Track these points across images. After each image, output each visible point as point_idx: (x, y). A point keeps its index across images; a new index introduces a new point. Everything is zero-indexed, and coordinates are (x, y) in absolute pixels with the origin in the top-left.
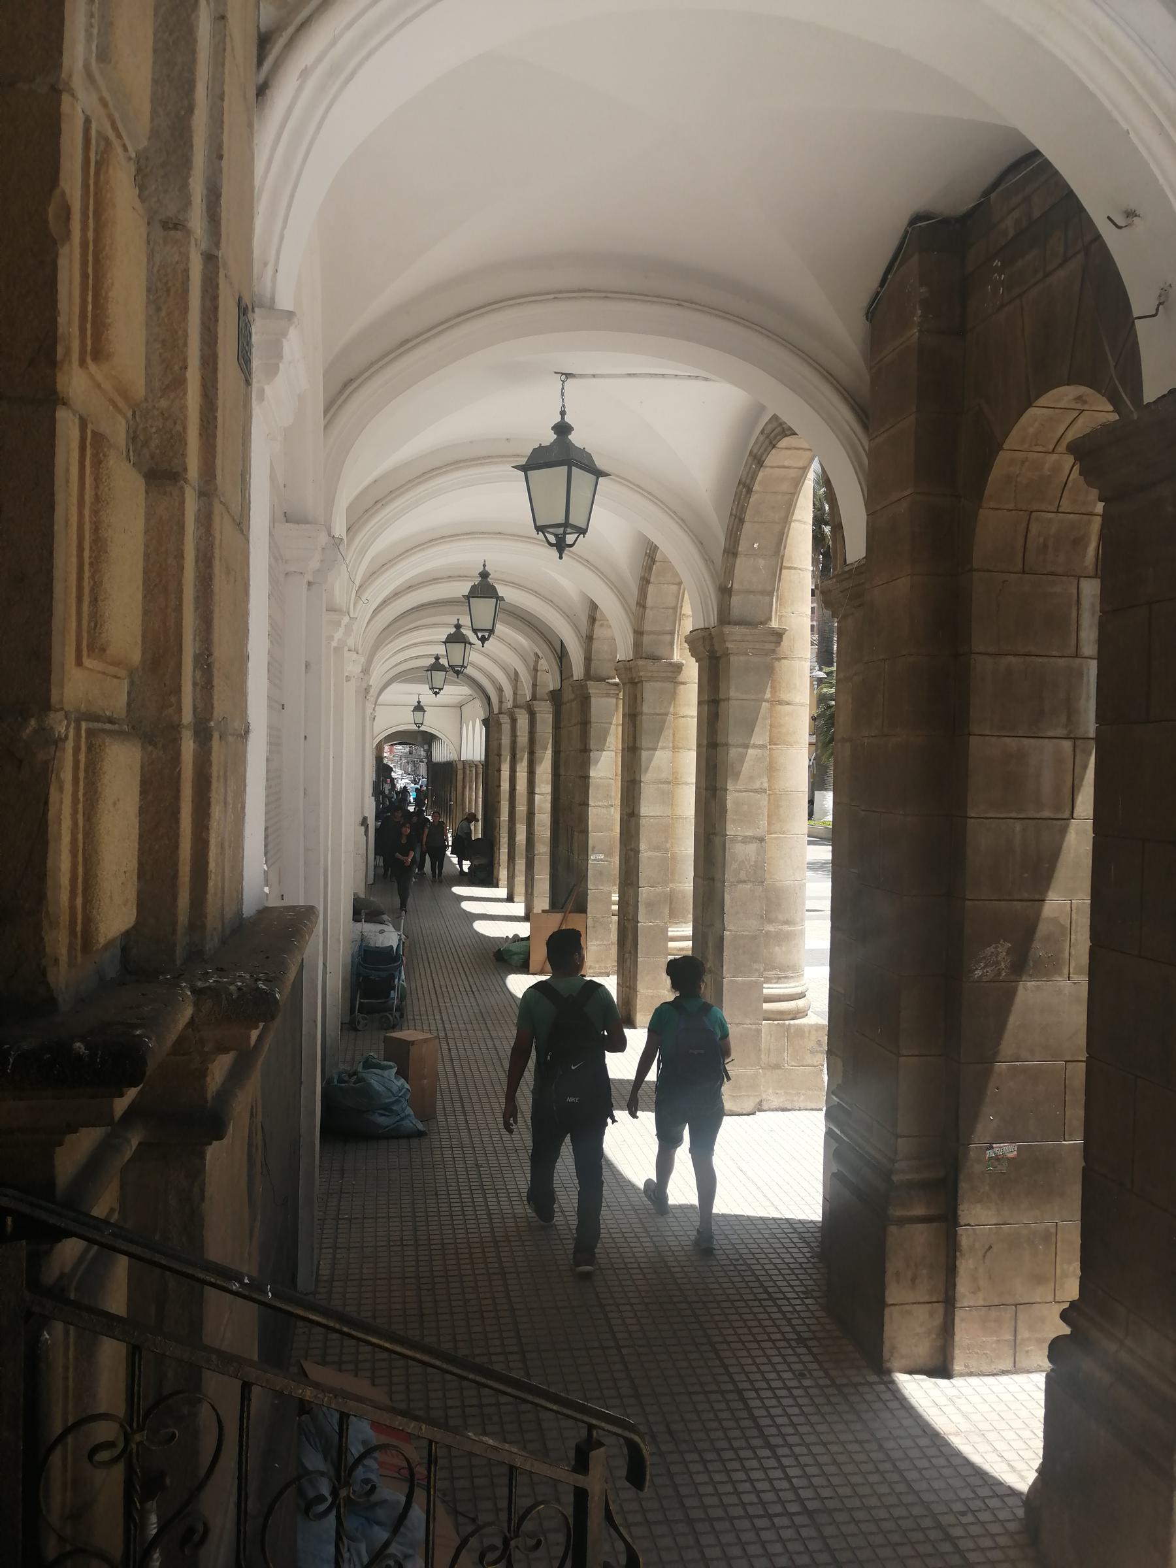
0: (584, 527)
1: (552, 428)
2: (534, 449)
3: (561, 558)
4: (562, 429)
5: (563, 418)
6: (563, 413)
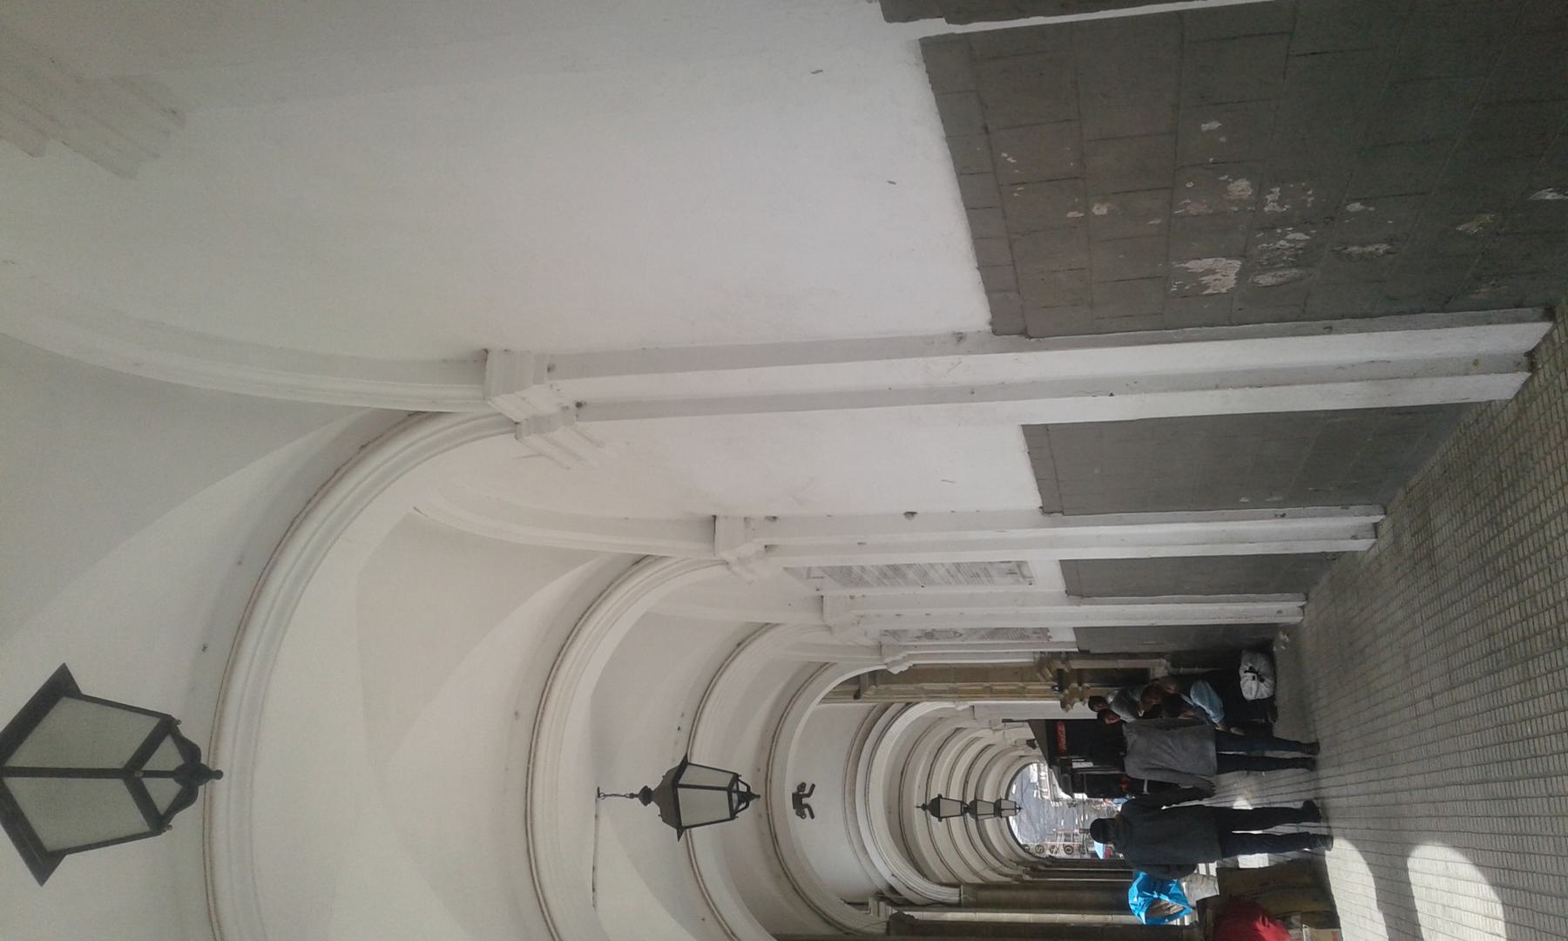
0: (731, 776)
1: (646, 805)
3: (759, 796)
4: (646, 796)
5: (636, 796)
6: (632, 796)
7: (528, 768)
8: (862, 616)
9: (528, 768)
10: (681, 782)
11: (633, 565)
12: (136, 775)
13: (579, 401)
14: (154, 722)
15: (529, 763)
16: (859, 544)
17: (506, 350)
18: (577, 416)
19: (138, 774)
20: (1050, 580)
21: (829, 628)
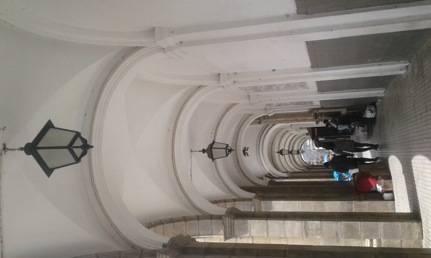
0: (226, 145)
1: (204, 153)
2: (209, 157)
3: (234, 150)
4: (204, 151)
5: (201, 151)
6: (200, 151)
7: (172, 145)
8: (261, 100)
9: (172, 145)
11: (197, 88)
12: (71, 148)
13: (181, 41)
14: (75, 134)
15: (173, 143)
16: (260, 79)
18: (180, 45)
19: (71, 147)
20: (314, 88)
21: (252, 104)
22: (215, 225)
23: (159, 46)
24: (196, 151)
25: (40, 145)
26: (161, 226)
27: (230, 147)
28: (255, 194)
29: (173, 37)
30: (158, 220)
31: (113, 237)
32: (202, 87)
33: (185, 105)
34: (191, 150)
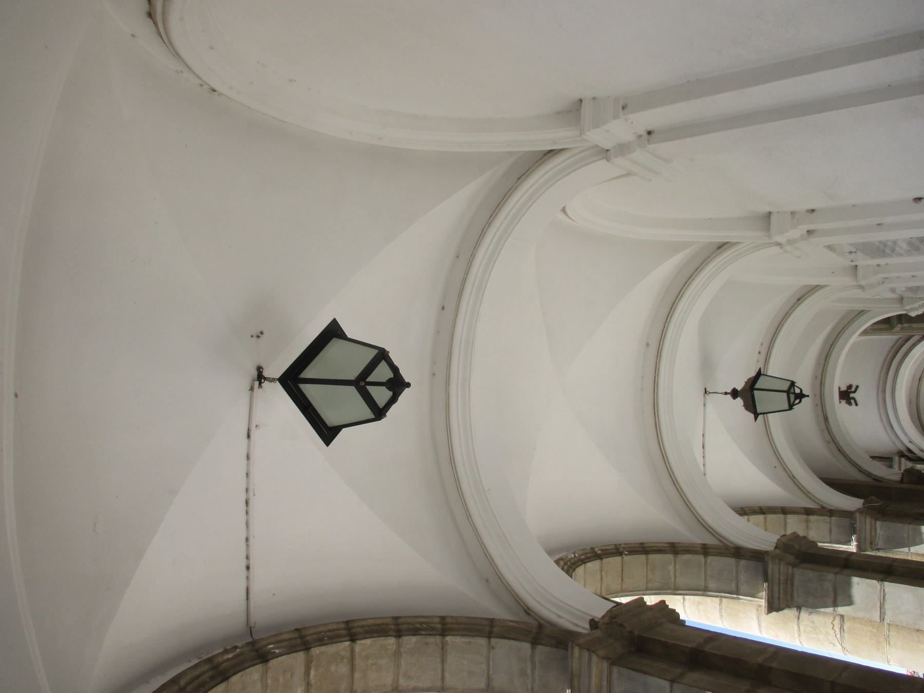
0: (789, 383)
3: (808, 396)
4: (735, 394)
6: (726, 393)
10: (757, 386)
13: (649, 129)
14: (375, 352)
15: (655, 374)
17: (594, 98)
18: (648, 141)
21: (861, 287)
22: (745, 572)
23: (597, 146)
24: (716, 393)
25: (308, 373)
26: (616, 558)
27: (798, 388)
28: (862, 501)
29: (626, 120)
30: (611, 545)
31: (487, 581)
32: (730, 245)
33: (686, 289)
34: (705, 389)
